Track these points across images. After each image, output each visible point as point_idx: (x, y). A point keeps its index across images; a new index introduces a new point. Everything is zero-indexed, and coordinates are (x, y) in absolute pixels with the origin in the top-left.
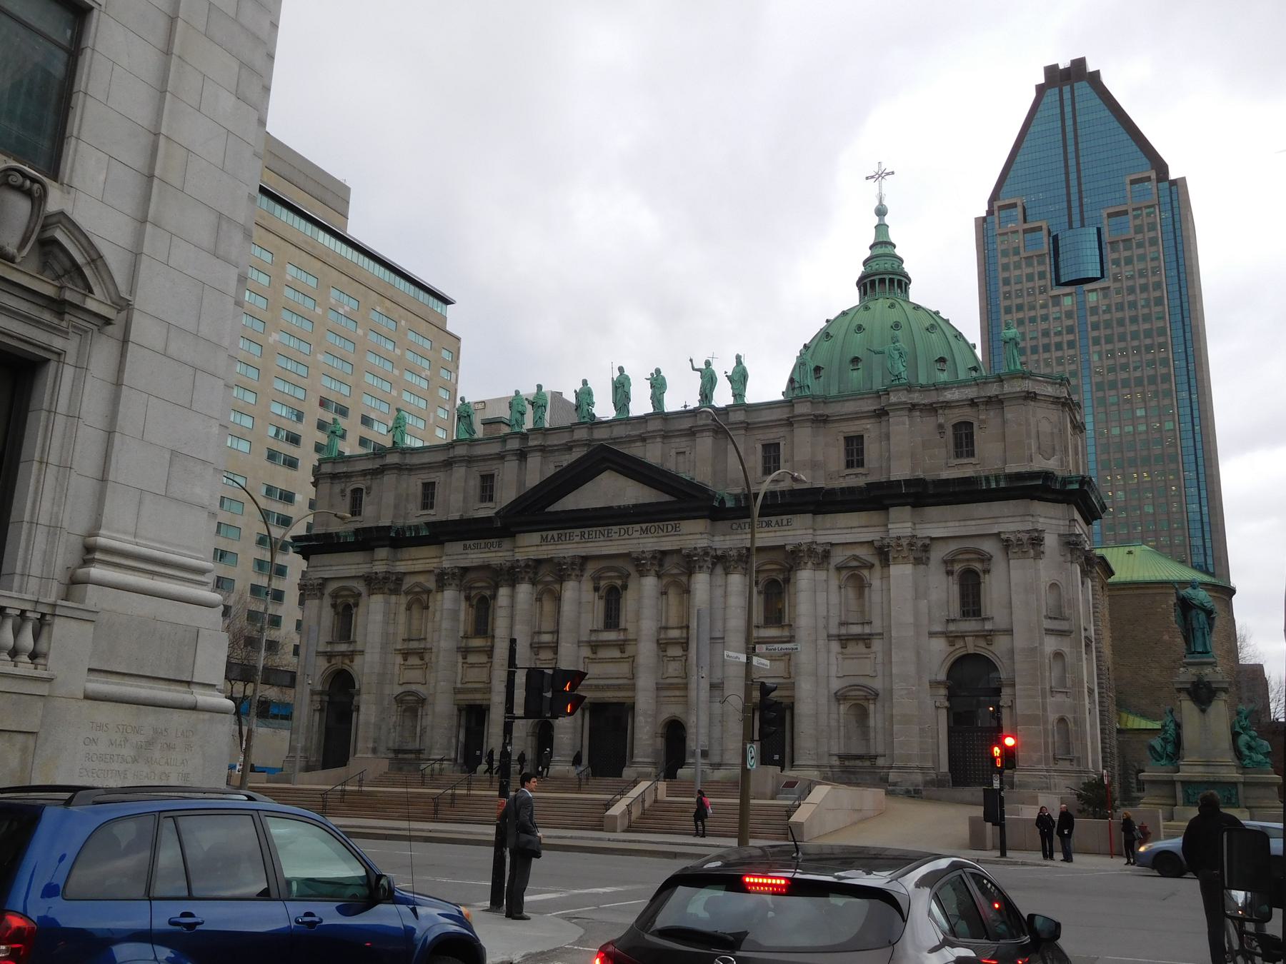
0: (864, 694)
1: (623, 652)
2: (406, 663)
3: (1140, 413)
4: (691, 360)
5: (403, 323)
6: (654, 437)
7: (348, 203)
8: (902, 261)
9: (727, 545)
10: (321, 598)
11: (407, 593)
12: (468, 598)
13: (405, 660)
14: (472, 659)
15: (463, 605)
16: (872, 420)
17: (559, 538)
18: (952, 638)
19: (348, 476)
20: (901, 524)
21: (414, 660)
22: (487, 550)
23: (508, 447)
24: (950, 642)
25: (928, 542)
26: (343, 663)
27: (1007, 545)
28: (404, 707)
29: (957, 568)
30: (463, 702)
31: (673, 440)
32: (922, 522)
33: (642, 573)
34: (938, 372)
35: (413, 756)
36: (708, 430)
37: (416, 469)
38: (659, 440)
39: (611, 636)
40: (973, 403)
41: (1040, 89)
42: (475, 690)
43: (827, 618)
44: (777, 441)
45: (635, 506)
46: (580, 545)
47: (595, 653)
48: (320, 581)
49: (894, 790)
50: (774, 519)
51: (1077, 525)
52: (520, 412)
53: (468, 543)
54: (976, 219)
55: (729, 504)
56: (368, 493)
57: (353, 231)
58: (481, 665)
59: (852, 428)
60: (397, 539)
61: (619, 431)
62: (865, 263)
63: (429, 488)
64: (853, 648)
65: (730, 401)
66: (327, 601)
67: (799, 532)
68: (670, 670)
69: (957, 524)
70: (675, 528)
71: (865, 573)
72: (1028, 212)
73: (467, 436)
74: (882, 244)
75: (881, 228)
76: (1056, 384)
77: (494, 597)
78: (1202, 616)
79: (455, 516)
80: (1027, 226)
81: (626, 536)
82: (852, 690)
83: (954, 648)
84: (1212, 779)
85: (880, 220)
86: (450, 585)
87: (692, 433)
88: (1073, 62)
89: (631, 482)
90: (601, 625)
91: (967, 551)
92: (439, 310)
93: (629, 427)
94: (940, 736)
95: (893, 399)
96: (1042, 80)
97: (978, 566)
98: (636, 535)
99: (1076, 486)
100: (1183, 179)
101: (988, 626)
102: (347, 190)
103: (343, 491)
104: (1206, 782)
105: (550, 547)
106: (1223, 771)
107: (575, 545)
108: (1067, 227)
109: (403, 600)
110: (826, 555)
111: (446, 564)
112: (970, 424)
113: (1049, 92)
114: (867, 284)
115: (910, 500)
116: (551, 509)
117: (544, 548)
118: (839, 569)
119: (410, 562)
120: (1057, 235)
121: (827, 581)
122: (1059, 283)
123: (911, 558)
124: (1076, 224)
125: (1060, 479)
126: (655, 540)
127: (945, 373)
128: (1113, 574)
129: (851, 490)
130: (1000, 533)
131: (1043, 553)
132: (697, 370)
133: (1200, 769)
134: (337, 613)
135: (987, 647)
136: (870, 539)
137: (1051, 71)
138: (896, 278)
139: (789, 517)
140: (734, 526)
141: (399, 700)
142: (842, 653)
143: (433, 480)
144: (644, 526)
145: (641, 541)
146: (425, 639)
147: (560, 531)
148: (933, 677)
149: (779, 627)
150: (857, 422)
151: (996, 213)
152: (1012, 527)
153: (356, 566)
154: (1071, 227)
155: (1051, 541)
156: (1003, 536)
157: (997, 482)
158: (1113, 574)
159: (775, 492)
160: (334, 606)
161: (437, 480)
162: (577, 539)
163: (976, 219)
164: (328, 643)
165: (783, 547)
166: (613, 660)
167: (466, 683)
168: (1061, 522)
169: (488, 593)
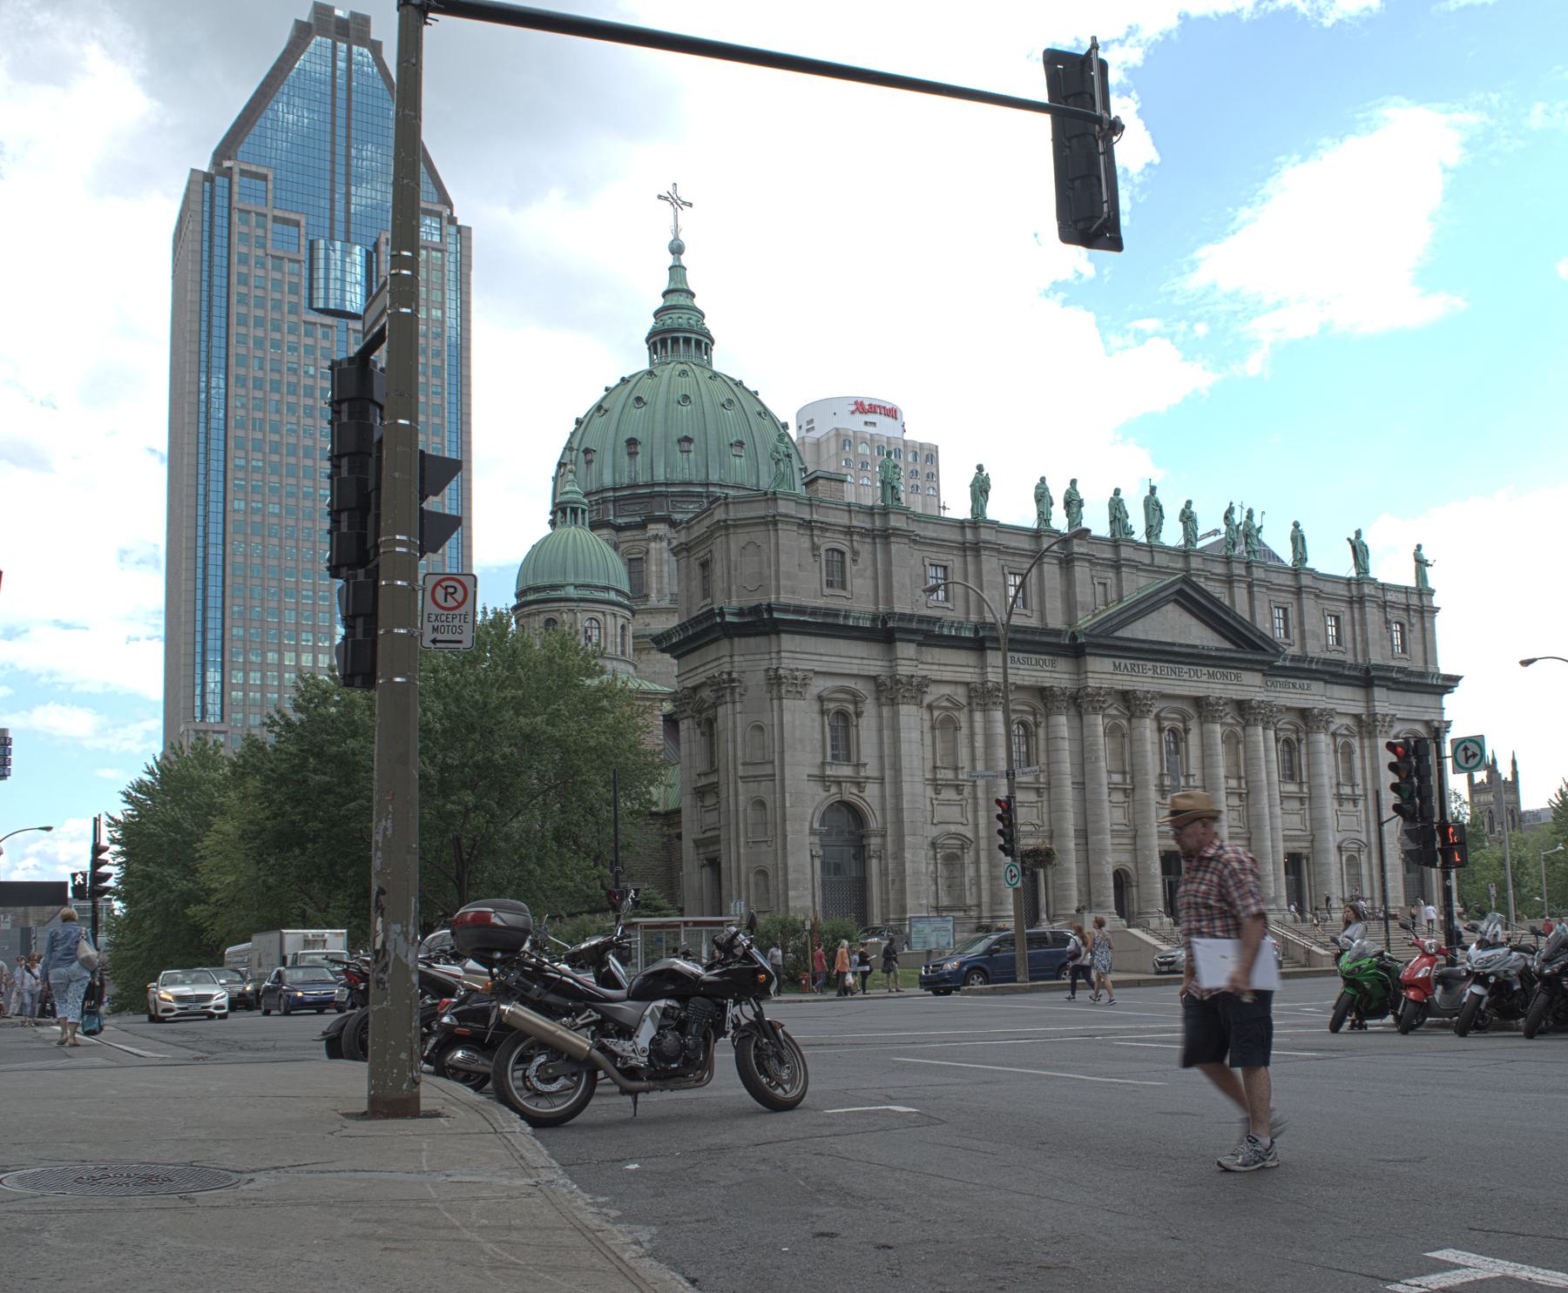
13: (937, 792)
35: (961, 914)
50: (1297, 681)
56: (855, 561)
70: (1237, 677)
74: (678, 290)
75: (677, 270)
98: (1205, 678)
105: (1125, 678)
110: (1328, 722)
116: (1119, 634)
117: (1119, 677)
118: (1334, 735)
119: (935, 667)
144: (1211, 670)
153: (859, 661)
160: (823, 712)
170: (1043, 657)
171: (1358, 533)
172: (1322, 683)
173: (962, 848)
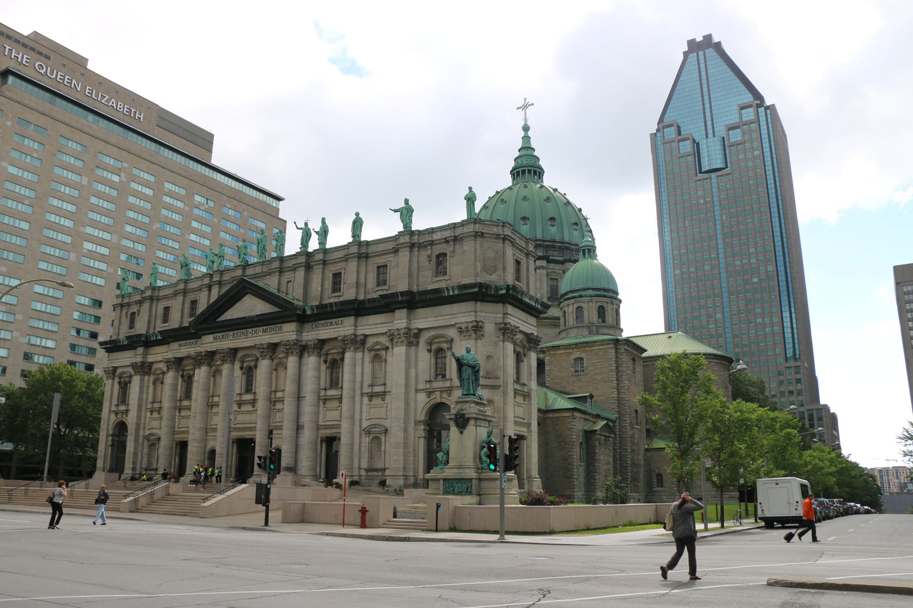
0: (379, 430)
1: (254, 407)
2: (152, 416)
3: (752, 250)
4: (295, 223)
5: (246, 213)
6: (275, 272)
7: (212, 143)
8: (538, 159)
9: (310, 338)
10: (113, 379)
11: (153, 374)
12: (182, 376)
14: (184, 413)
15: (180, 380)
16: (393, 255)
17: (222, 337)
18: (430, 393)
19: (129, 305)
20: (399, 320)
21: (155, 415)
22: (190, 346)
23: (204, 283)
24: (427, 395)
25: (416, 331)
26: (122, 417)
27: (460, 331)
28: (150, 443)
29: (434, 347)
30: (178, 440)
31: (286, 274)
32: (415, 319)
33: (263, 357)
34: (550, 227)
36: (302, 266)
37: (162, 299)
38: (277, 274)
39: (248, 397)
40: (447, 241)
41: (686, 54)
42: (184, 432)
43: (362, 382)
44: (340, 271)
45: (257, 316)
46: (232, 342)
47: (239, 408)
48: (111, 369)
49: (388, 490)
50: (334, 321)
51: (509, 316)
52: (211, 261)
53: (181, 342)
54: (651, 134)
55: (309, 312)
56: (138, 315)
57: (215, 161)
58: (188, 417)
59: (380, 261)
60: (147, 342)
61: (258, 270)
62: (515, 160)
63: (167, 309)
64: (377, 401)
65: (317, 247)
66: (117, 380)
67: (346, 328)
68: (277, 417)
69: (434, 319)
70: (280, 328)
71: (384, 352)
72: (682, 129)
73: (186, 278)
74: (527, 148)
75: (526, 138)
76: (500, 226)
77: (194, 375)
78: (469, 371)
79: (177, 326)
80: (680, 137)
81: (255, 335)
82: (372, 428)
83: (430, 399)
84: (458, 477)
85: (525, 134)
86: (172, 368)
87: (294, 268)
88: (704, 37)
89: (259, 301)
90: (243, 391)
91: (438, 337)
92: (274, 205)
93: (264, 267)
94: (420, 456)
95: (402, 240)
96: (686, 49)
97: (445, 346)
98: (260, 334)
99: (504, 292)
100: (774, 105)
101: (448, 384)
102: (211, 136)
103: (127, 313)
104: (457, 479)
106: (467, 472)
107: (230, 342)
108: (705, 137)
109: (152, 378)
110: (363, 342)
111: (170, 355)
112: (445, 255)
113: (690, 55)
114: (516, 173)
115: (406, 305)
116: (218, 320)
117: (215, 344)
118: (370, 350)
119: (155, 356)
120: (698, 143)
121: (363, 359)
122: (701, 172)
123: (405, 341)
124: (710, 135)
125: (493, 287)
126: (269, 336)
127: (555, 227)
128: (645, 351)
129: (373, 300)
130: (456, 323)
131: (483, 335)
132: (300, 229)
133: (456, 471)
134: (122, 388)
135: (448, 398)
136: (385, 332)
137: (692, 44)
138: (532, 169)
139: (342, 319)
140: (314, 326)
141: (147, 438)
142: (369, 404)
143: (169, 305)
144: (264, 328)
145: (262, 337)
146: (161, 402)
147: (223, 333)
148: (418, 418)
149: (336, 389)
150: (384, 257)
151: (661, 130)
152: (463, 320)
154: (707, 137)
155: (489, 328)
156: (457, 326)
157: (453, 291)
158: (645, 351)
159: (332, 303)
160: (119, 383)
161: (171, 305)
162: (231, 338)
163: (651, 134)
164: (117, 405)
165: (336, 339)
166: (249, 412)
167: (180, 428)
168: (498, 316)
169: (191, 372)
170: (192, 341)
171: (407, 201)
172: (353, 318)
173: (156, 439)
